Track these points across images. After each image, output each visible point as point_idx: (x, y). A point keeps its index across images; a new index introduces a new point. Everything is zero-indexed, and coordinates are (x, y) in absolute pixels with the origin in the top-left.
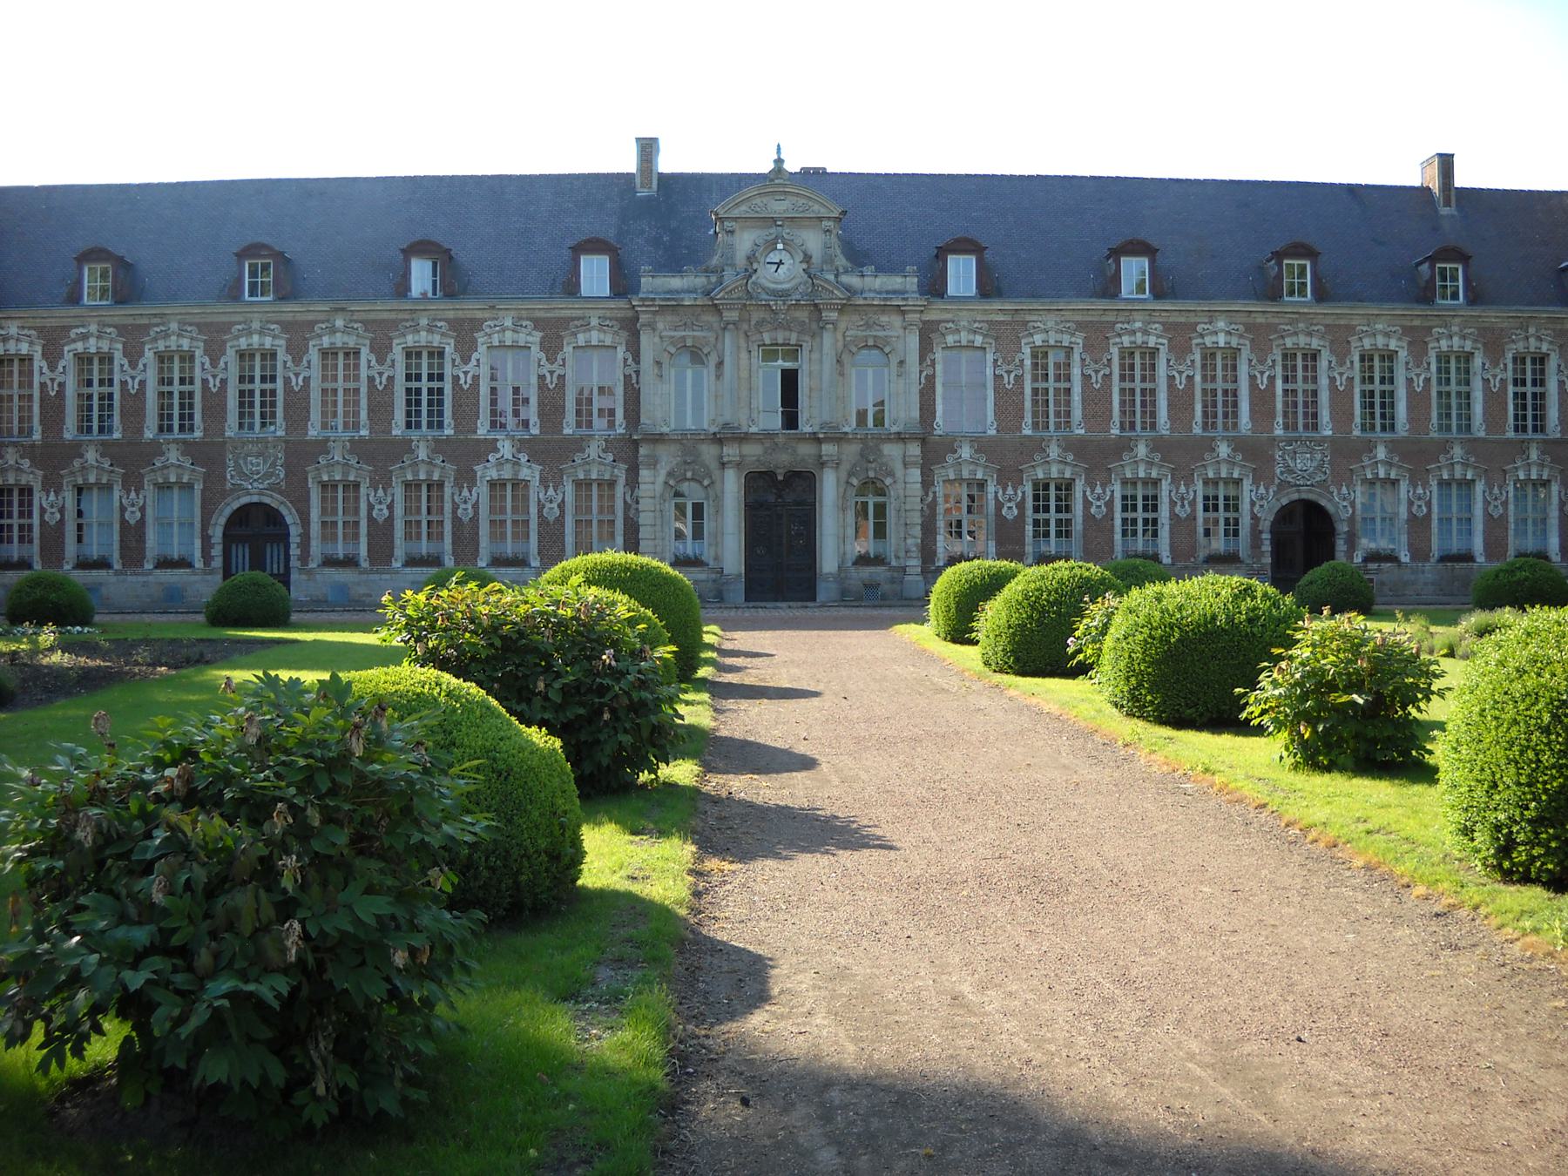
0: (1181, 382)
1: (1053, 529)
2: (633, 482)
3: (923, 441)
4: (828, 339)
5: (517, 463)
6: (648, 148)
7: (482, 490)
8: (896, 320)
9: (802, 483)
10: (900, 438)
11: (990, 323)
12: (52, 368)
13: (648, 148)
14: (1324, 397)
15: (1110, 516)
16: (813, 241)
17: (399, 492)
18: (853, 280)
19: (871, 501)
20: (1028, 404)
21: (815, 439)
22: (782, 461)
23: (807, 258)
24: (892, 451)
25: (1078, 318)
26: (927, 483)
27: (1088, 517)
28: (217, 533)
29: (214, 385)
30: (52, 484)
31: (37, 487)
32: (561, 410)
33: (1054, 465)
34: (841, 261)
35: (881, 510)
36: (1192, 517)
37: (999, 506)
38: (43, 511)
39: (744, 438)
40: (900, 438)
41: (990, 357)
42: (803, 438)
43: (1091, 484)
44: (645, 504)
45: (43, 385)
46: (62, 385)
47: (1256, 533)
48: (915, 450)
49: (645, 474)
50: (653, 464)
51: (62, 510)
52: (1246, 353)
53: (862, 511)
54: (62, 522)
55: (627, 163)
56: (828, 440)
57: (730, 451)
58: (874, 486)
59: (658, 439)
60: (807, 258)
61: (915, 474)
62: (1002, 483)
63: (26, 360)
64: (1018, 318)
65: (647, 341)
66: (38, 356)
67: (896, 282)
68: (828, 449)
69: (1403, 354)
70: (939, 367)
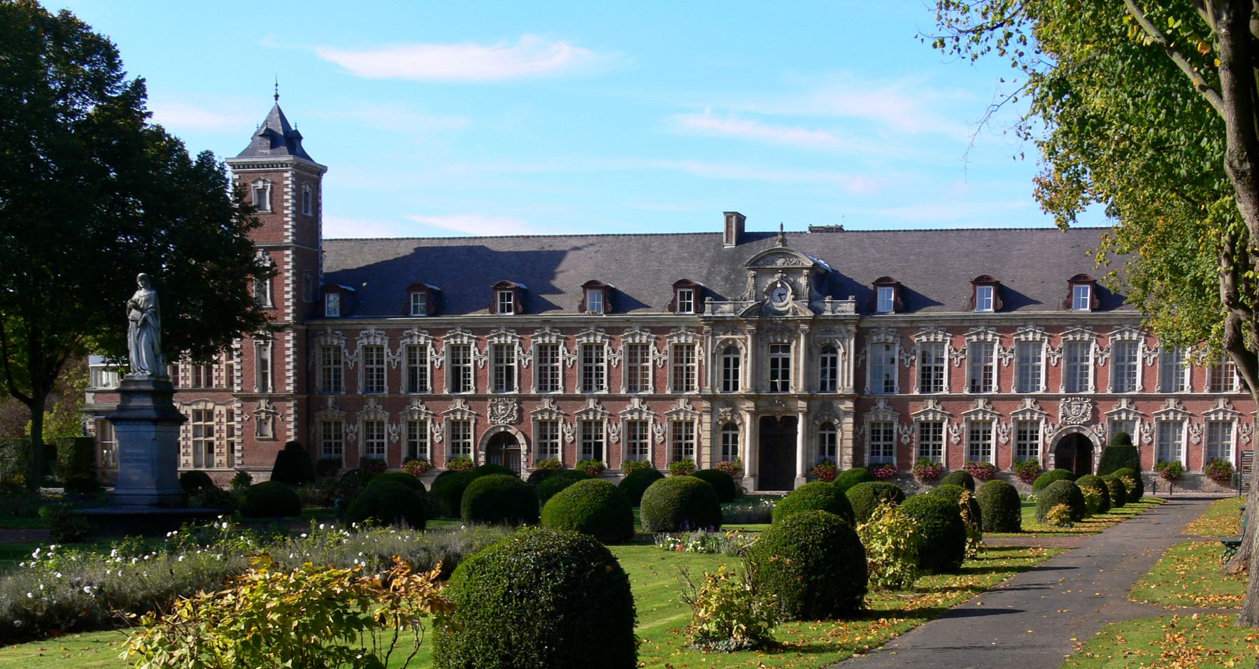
1: (882, 451)
5: (641, 412)
11: (899, 328)
12: (394, 353)
25: (948, 324)
26: (858, 423)
30: (394, 420)
31: (386, 420)
37: (899, 436)
38: (389, 434)
41: (897, 349)
45: (389, 363)
46: (399, 363)
51: (399, 435)
54: (399, 441)
63: (380, 349)
64: (914, 325)
66: (386, 346)
70: (869, 355)
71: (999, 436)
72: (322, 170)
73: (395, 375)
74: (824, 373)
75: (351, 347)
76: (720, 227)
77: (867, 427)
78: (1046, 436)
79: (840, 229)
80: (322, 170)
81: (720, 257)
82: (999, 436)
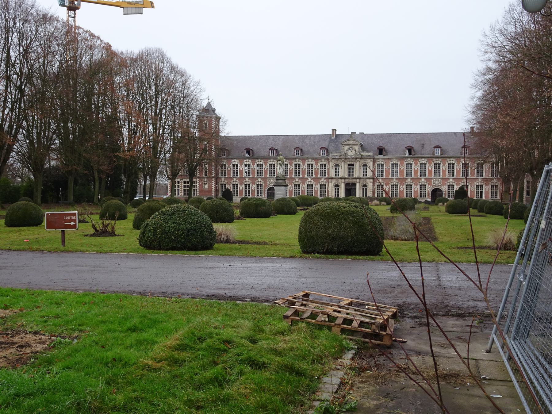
0: (416, 169)
2: (328, 185)
3: (373, 179)
4: (358, 163)
6: (334, 130)
7: (306, 186)
8: (369, 160)
9: (354, 185)
10: (369, 178)
13: (334, 130)
14: (441, 171)
15: (404, 190)
16: (357, 148)
17: (293, 186)
18: (362, 154)
19: (365, 188)
20: (391, 173)
21: (356, 178)
22: (351, 181)
23: (355, 151)
24: (368, 180)
26: (374, 185)
27: (400, 191)
28: (266, 192)
29: (266, 169)
32: (318, 173)
33: (395, 182)
34: (361, 151)
35: (366, 189)
36: (417, 191)
39: (345, 178)
40: (369, 178)
42: (354, 178)
43: (400, 185)
44: (330, 188)
47: (428, 194)
48: (372, 180)
49: (330, 184)
50: (331, 182)
52: (427, 164)
53: (363, 189)
55: (330, 133)
56: (358, 178)
57: (343, 180)
58: (365, 186)
59: (332, 178)
60: (355, 151)
61: (372, 184)
62: (386, 185)
63: (237, 165)
65: (330, 163)
67: (369, 154)
68: (358, 180)
69: (456, 164)
71: (416, 188)
72: (220, 118)
73: (304, 172)
74: (336, 172)
75: (229, 164)
76: (330, 133)
77: (376, 186)
78: (429, 189)
79: (363, 133)
80: (220, 118)
81: (331, 141)
82: (416, 188)
